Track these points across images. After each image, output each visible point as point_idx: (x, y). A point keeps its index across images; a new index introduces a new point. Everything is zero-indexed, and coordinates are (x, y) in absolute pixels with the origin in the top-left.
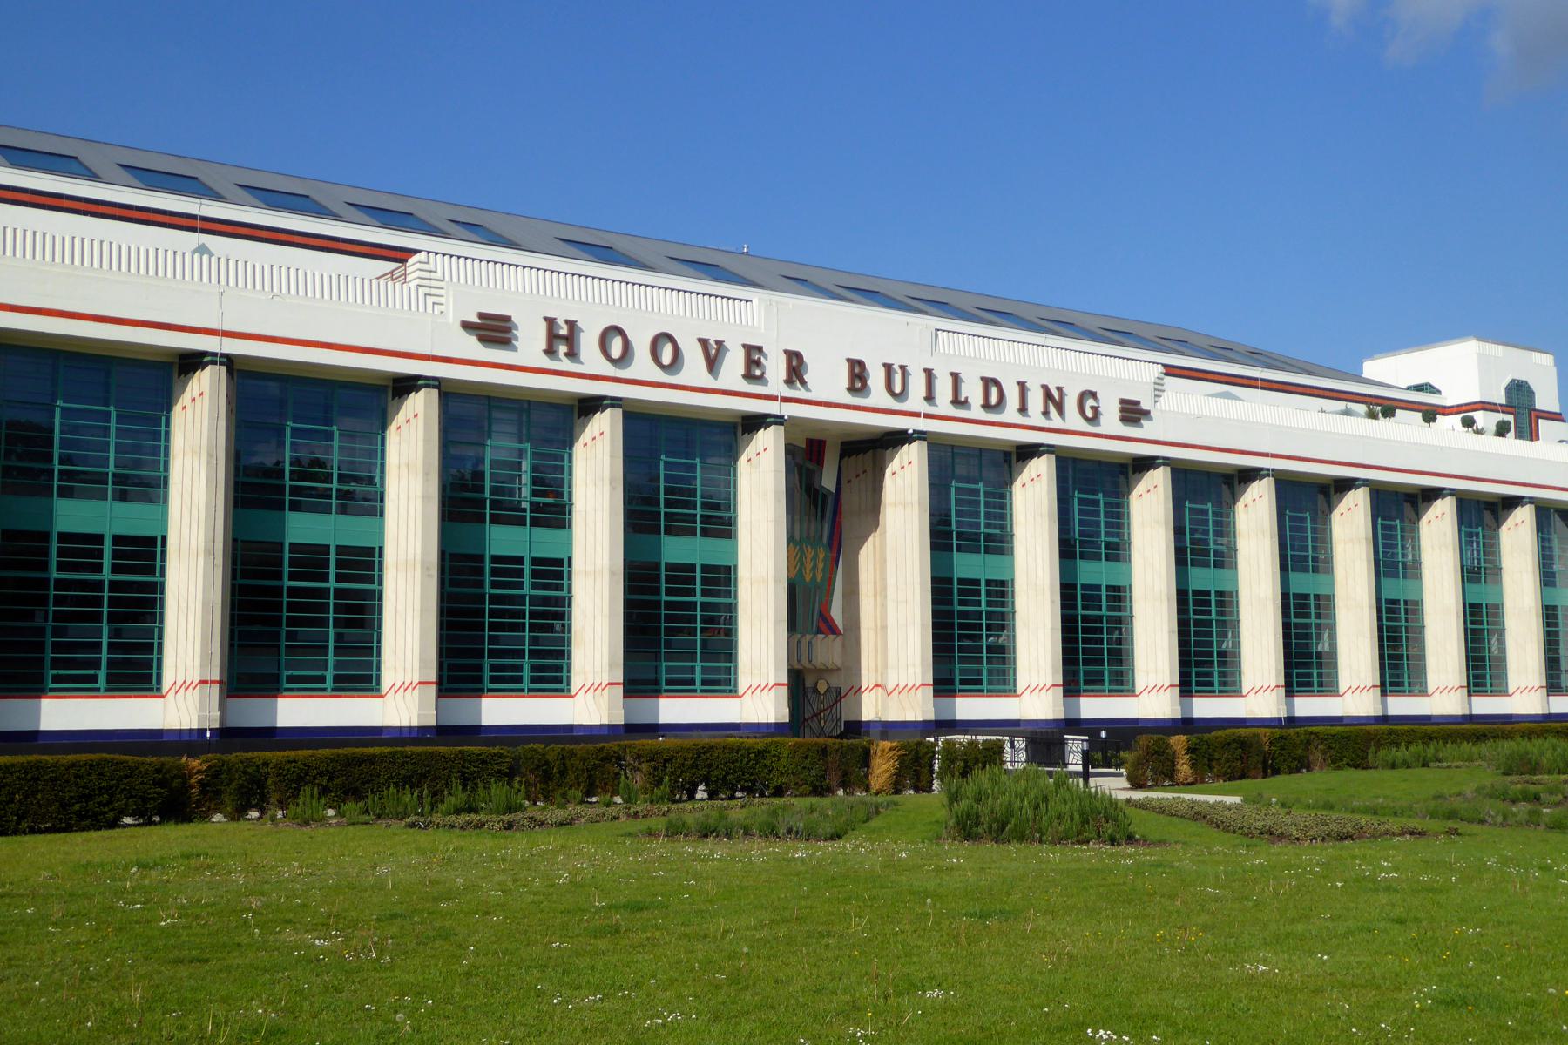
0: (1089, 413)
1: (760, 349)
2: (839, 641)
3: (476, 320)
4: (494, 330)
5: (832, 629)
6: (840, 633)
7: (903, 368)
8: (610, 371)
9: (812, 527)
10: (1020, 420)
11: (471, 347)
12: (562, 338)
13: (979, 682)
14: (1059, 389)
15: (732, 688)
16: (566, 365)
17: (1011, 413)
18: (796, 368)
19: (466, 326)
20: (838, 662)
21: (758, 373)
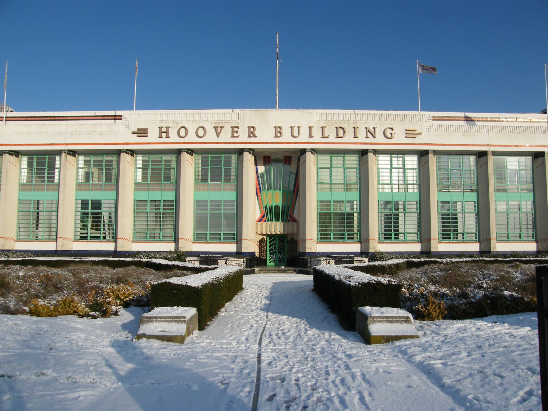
0: (389, 136)
2: (295, 224)
3: (136, 130)
4: (142, 132)
5: (294, 220)
7: (298, 127)
8: (181, 140)
10: (355, 140)
11: (135, 139)
12: (164, 132)
14: (374, 128)
16: (164, 140)
17: (349, 137)
18: (252, 132)
19: (133, 133)
20: (295, 232)
21: (236, 134)
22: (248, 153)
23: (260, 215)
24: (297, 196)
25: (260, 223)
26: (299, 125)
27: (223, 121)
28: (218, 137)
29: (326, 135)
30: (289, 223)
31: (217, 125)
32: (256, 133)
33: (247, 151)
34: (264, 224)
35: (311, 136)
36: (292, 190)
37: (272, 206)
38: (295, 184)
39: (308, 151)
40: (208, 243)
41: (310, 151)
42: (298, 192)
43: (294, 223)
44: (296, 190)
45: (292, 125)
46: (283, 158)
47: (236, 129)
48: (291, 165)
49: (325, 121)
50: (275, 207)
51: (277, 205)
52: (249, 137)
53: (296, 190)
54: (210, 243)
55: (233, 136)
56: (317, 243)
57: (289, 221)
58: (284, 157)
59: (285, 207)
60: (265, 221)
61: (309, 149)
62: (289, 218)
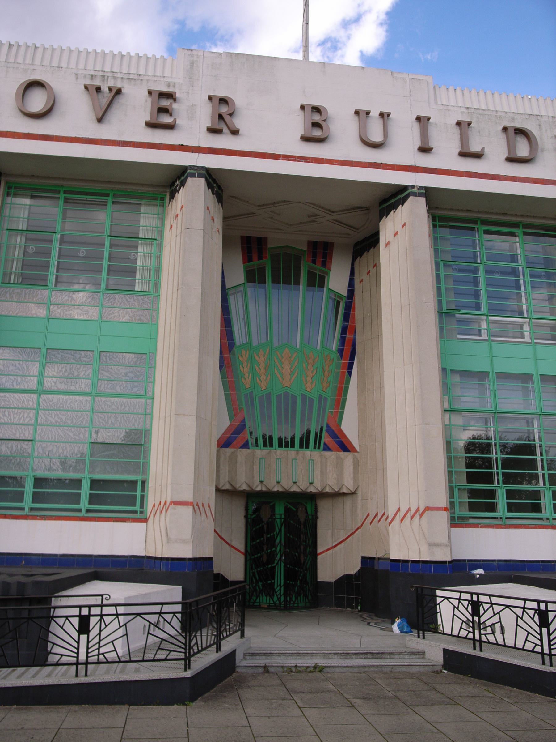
1: (169, 96)
2: (348, 458)
6: (354, 450)
9: (252, 308)
13: (537, 508)
15: (137, 508)
20: (348, 485)
21: (166, 119)
22: (203, 180)
23: (229, 424)
24: (350, 367)
25: (229, 451)
26: (385, 110)
27: (119, 75)
28: (100, 120)
29: (475, 148)
30: (327, 454)
31: (97, 83)
32: (238, 122)
33: (200, 176)
34: (242, 454)
35: (425, 150)
36: (335, 345)
37: (269, 396)
38: (344, 331)
39: (415, 194)
40: (25, 517)
41: (420, 195)
42: (353, 353)
43: (342, 454)
44: (348, 348)
45: (363, 107)
46: (305, 249)
47: (165, 103)
48: (330, 269)
49: (465, 111)
50: (279, 397)
51: (286, 394)
52: (213, 131)
53: (348, 348)
54: (34, 518)
55: (151, 125)
56: (453, 526)
57: (327, 448)
58: (309, 243)
59: (311, 400)
60: (246, 445)
61: (420, 188)
62: (326, 438)
